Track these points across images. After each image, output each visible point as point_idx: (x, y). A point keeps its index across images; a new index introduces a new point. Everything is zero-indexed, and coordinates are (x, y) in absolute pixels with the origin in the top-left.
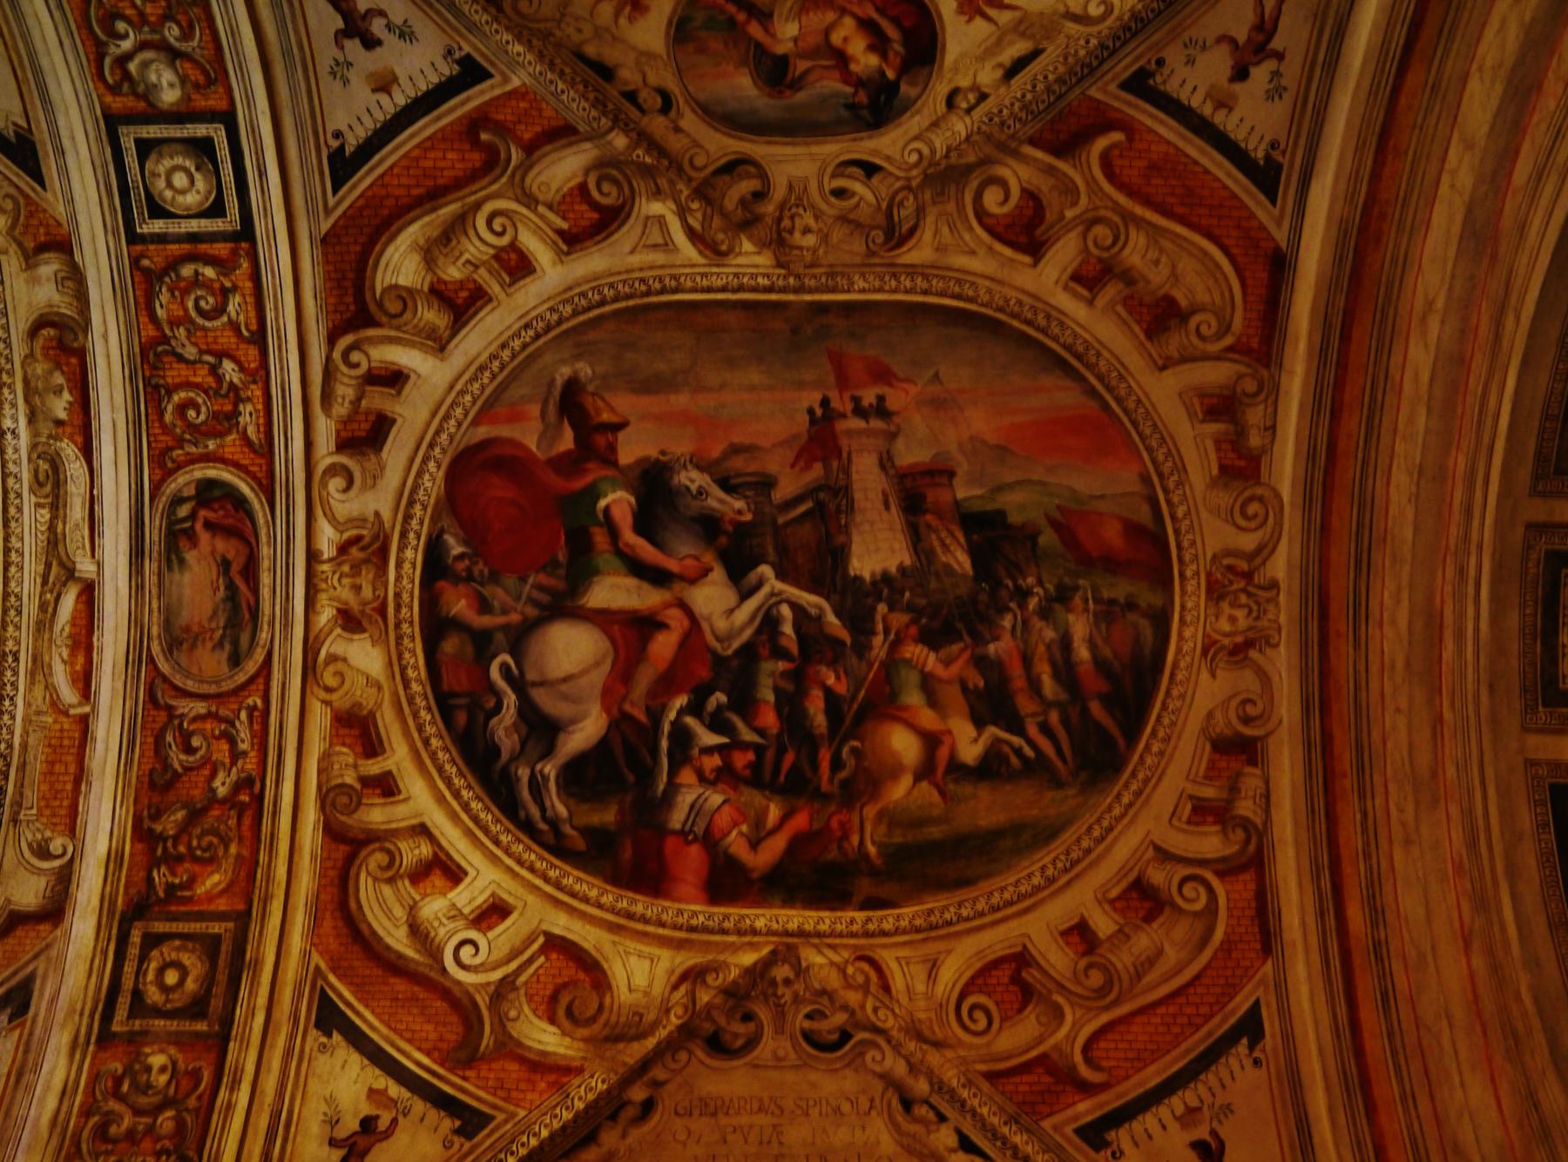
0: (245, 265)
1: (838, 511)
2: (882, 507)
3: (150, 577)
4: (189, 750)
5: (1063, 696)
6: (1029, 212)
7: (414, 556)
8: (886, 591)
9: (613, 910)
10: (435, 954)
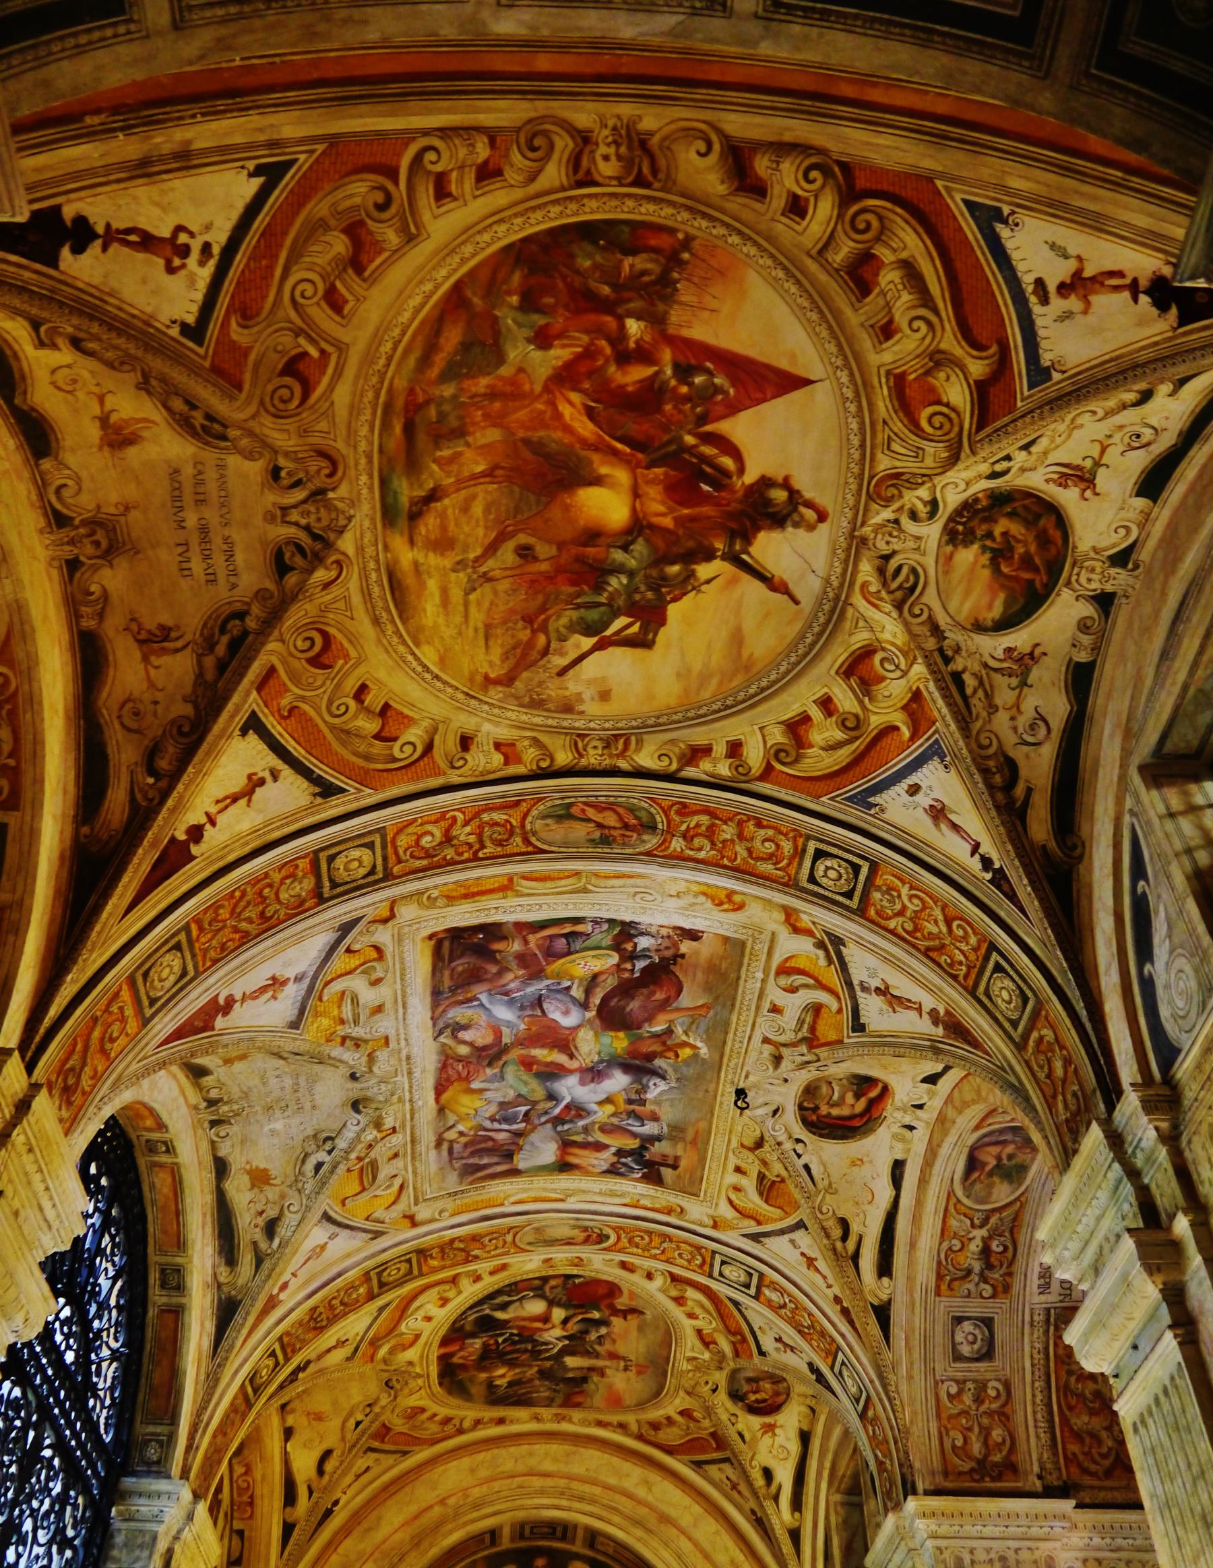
7: (575, 1271)
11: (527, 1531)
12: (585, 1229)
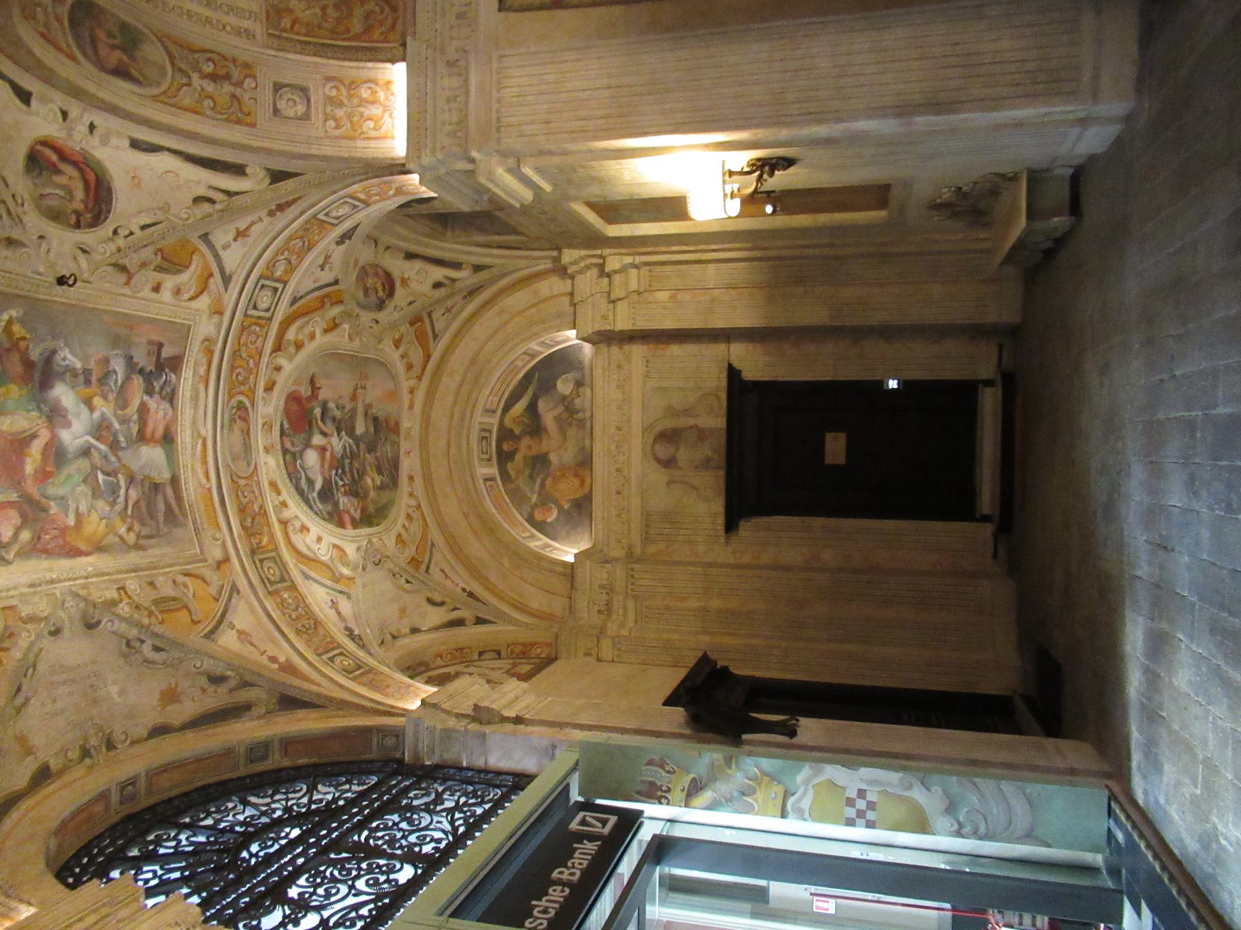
7: (278, 428)
11: (486, 456)
12: (232, 421)
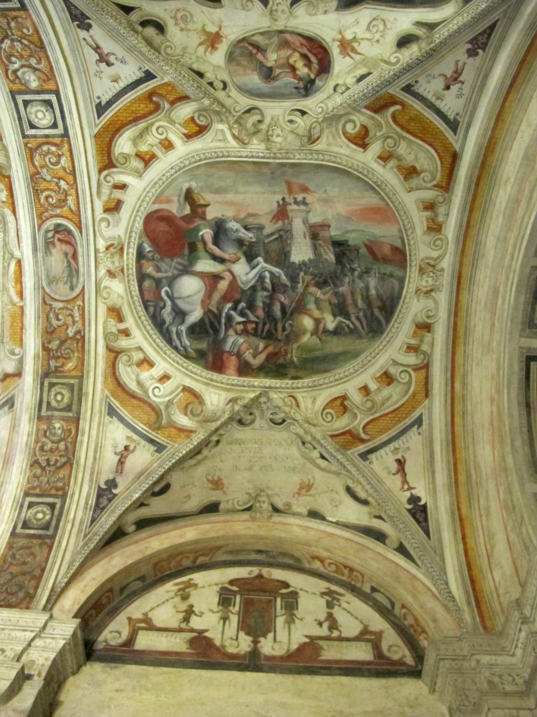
0: (66, 146)
1: (287, 239)
2: (303, 237)
3: (40, 259)
4: (58, 319)
5: (365, 307)
6: (363, 133)
8: (304, 268)
9: (205, 378)
10: (146, 392)
